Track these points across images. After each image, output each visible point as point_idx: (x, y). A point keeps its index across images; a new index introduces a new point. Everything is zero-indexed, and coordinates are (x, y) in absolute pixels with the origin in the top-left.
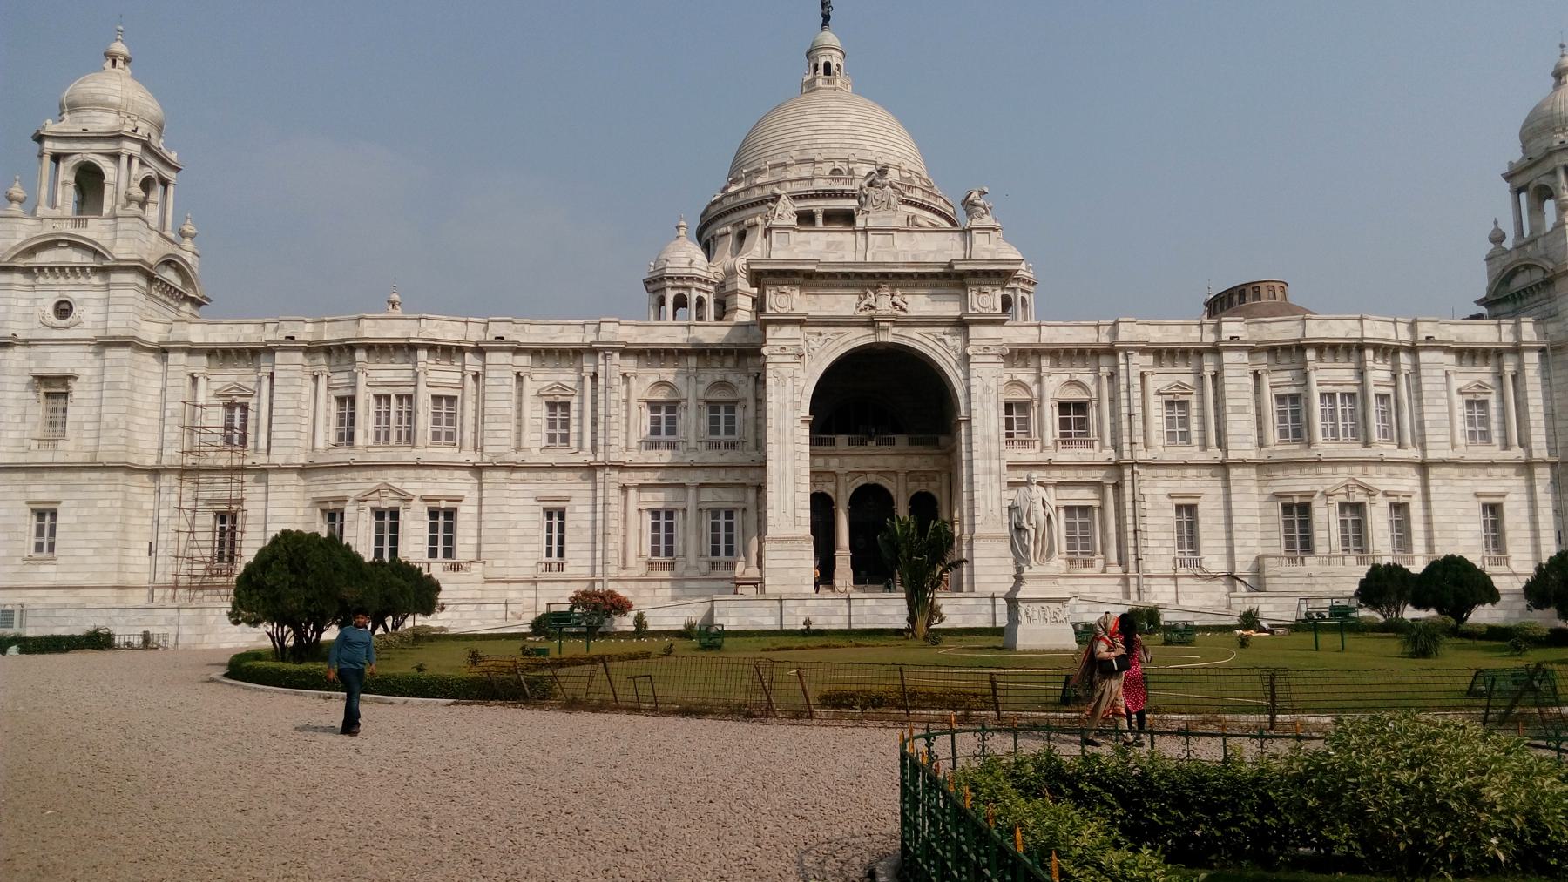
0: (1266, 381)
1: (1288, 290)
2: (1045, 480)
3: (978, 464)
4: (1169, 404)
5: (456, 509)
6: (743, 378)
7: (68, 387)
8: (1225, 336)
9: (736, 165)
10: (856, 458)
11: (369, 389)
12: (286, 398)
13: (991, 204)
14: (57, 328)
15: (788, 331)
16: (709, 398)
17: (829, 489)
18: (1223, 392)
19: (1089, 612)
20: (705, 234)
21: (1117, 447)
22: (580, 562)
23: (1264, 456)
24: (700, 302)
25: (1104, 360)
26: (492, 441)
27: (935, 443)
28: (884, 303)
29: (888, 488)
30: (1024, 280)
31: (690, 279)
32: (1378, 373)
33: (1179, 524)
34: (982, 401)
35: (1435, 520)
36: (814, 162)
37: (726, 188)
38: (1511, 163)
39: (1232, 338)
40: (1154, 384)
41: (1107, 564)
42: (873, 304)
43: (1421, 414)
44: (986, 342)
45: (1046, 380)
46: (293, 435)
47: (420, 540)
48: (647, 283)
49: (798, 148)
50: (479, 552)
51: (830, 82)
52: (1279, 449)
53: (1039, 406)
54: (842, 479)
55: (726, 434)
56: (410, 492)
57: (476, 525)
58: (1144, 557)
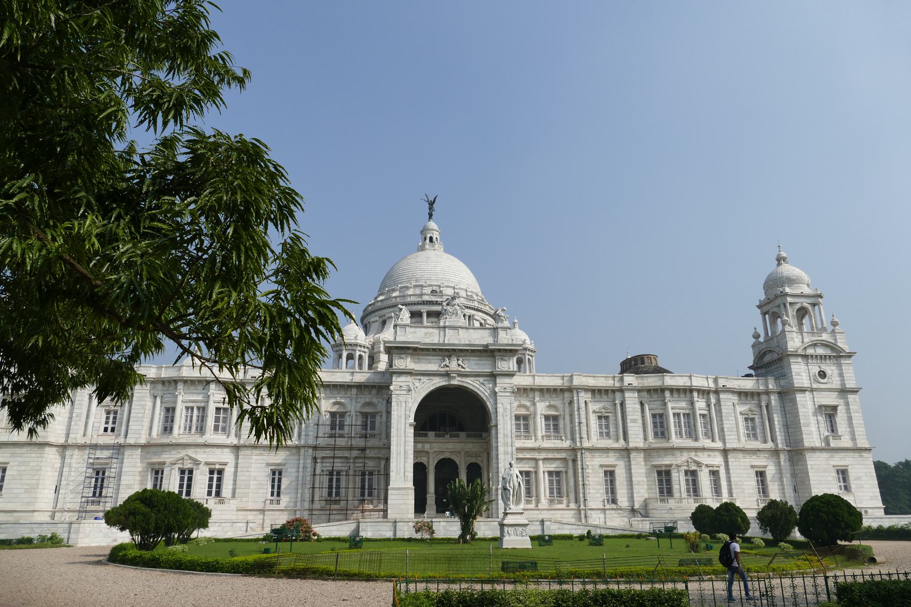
0: (647, 407)
1: (658, 359)
2: (537, 457)
3: (501, 449)
4: (600, 418)
5: (224, 469)
6: (381, 400)
8: (626, 384)
9: (383, 286)
10: (439, 444)
12: (137, 407)
13: (508, 316)
15: (403, 378)
16: (362, 411)
17: (424, 460)
18: (626, 412)
19: (559, 529)
20: (365, 321)
21: (573, 439)
23: (647, 446)
24: (360, 357)
25: (567, 395)
27: (480, 436)
28: (453, 365)
30: (529, 350)
31: (356, 345)
32: (700, 404)
33: (606, 481)
35: (732, 479)
36: (422, 286)
37: (377, 297)
38: (760, 300)
41: (569, 502)
42: (448, 364)
43: (722, 424)
44: (505, 386)
45: (538, 404)
47: (203, 486)
51: (433, 246)
55: (371, 430)
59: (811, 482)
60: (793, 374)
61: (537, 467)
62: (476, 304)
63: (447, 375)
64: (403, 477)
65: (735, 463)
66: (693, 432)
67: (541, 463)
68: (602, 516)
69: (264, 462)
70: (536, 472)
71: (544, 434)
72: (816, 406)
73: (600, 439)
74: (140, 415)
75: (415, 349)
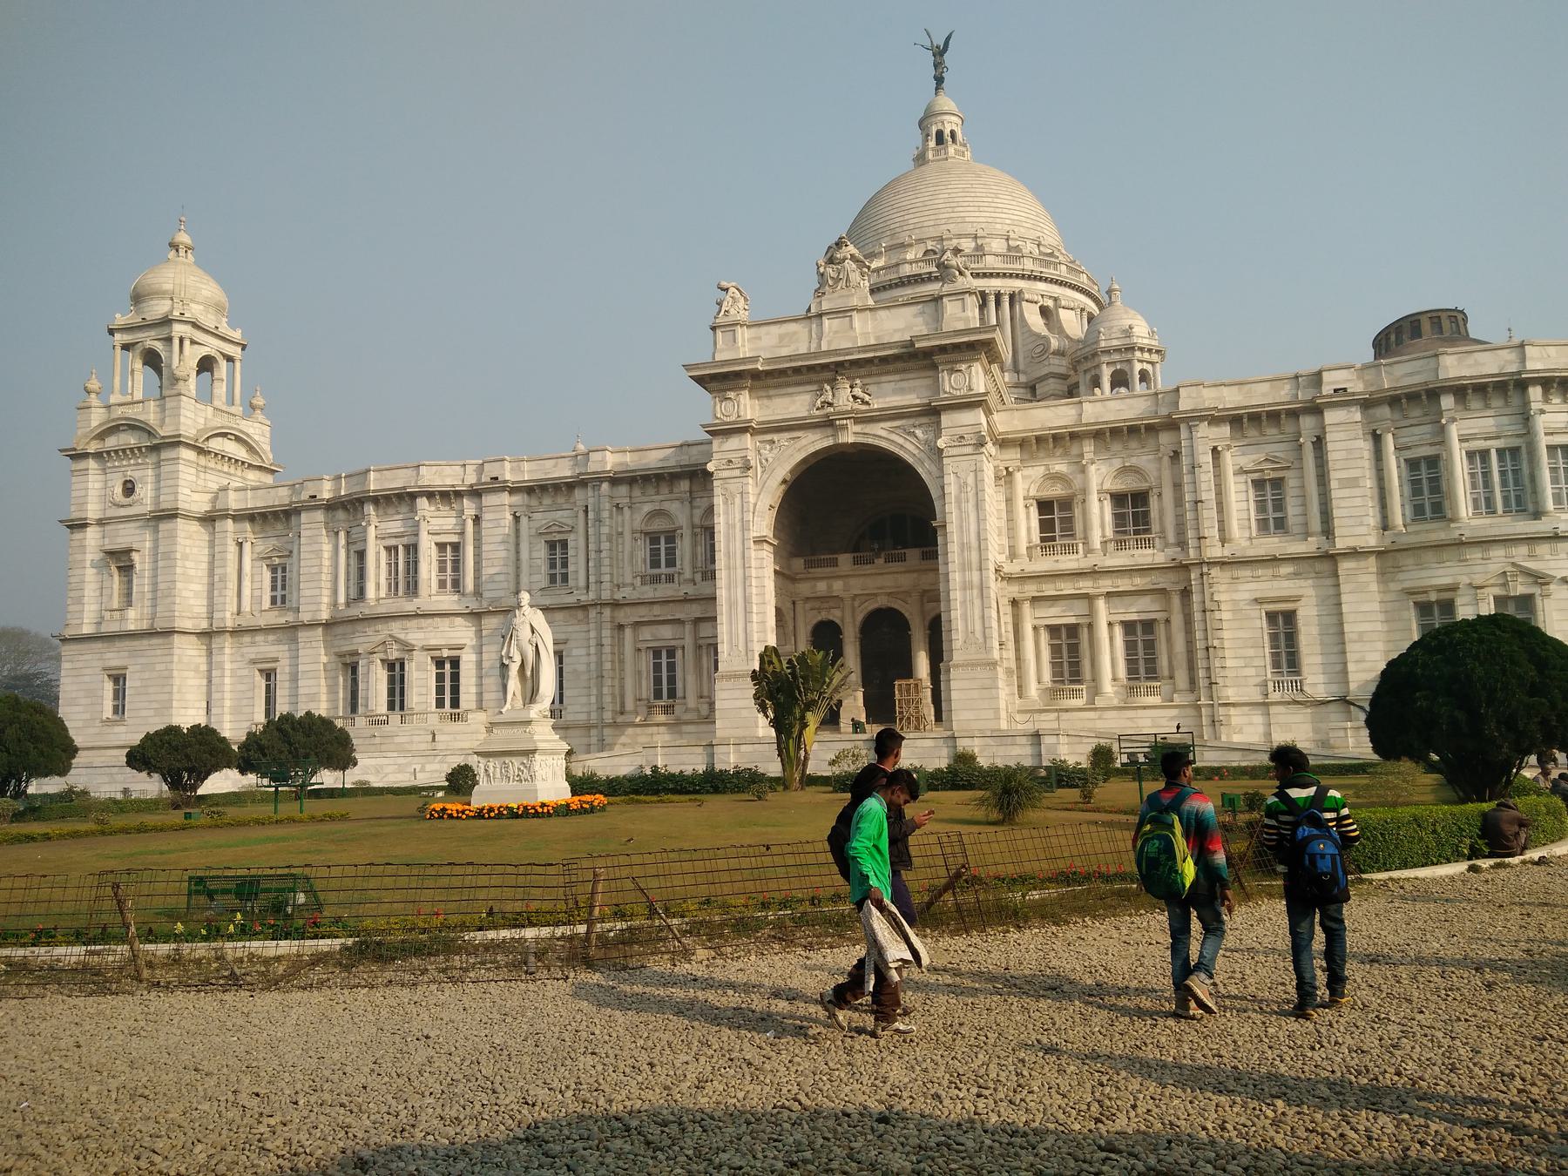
0: (1389, 442)
2: (1090, 591)
3: (956, 578)
4: (1258, 484)
7: (132, 561)
11: (379, 542)
14: (123, 506)
17: (835, 615)
21: (1182, 544)
22: (577, 708)
25: (1165, 438)
26: (490, 586)
28: (843, 397)
34: (958, 501)
39: (1335, 391)
40: (1230, 461)
44: (960, 431)
49: (888, 233)
54: (848, 603)
56: (413, 642)
61: (1092, 613)
62: (1028, 265)
63: (828, 424)
64: (743, 653)
66: (1528, 497)
68: (1258, 719)
70: (1090, 626)
71: (1109, 533)
74: (315, 570)
75: (756, 375)
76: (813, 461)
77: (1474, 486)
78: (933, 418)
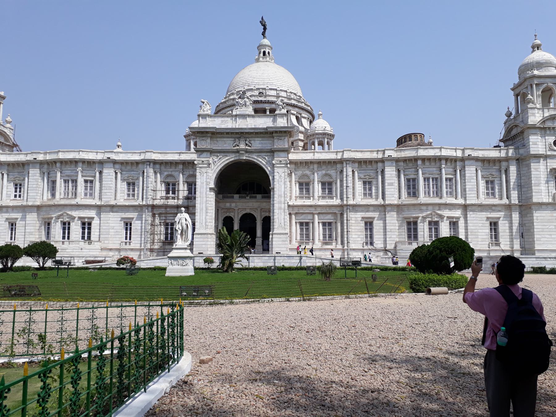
3: (276, 206)
10: (242, 203)
16: (187, 181)
17: (231, 215)
21: (342, 199)
25: (339, 166)
29: (254, 214)
35: (469, 228)
38: (514, 84)
41: (337, 244)
46: (35, 194)
48: (185, 136)
50: (99, 238)
52: (405, 199)
53: (313, 183)
57: (98, 227)
58: (350, 242)
59: (535, 230)
60: (531, 143)
61: (313, 219)
63: (238, 152)
64: (204, 226)
65: (472, 216)
66: (439, 192)
67: (316, 216)
69: (119, 216)
70: (313, 223)
72: (549, 170)
73: (364, 199)
75: (213, 133)
76: (231, 163)
77: (425, 188)
78: (271, 154)
